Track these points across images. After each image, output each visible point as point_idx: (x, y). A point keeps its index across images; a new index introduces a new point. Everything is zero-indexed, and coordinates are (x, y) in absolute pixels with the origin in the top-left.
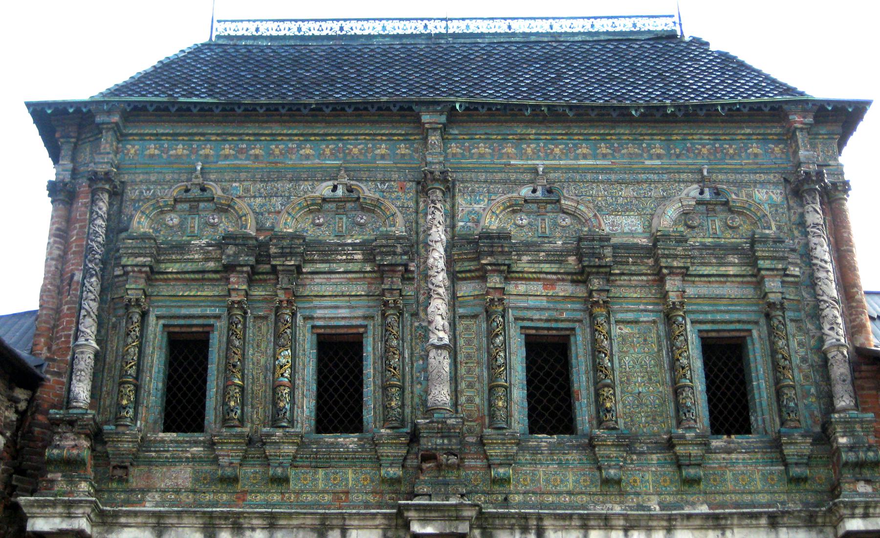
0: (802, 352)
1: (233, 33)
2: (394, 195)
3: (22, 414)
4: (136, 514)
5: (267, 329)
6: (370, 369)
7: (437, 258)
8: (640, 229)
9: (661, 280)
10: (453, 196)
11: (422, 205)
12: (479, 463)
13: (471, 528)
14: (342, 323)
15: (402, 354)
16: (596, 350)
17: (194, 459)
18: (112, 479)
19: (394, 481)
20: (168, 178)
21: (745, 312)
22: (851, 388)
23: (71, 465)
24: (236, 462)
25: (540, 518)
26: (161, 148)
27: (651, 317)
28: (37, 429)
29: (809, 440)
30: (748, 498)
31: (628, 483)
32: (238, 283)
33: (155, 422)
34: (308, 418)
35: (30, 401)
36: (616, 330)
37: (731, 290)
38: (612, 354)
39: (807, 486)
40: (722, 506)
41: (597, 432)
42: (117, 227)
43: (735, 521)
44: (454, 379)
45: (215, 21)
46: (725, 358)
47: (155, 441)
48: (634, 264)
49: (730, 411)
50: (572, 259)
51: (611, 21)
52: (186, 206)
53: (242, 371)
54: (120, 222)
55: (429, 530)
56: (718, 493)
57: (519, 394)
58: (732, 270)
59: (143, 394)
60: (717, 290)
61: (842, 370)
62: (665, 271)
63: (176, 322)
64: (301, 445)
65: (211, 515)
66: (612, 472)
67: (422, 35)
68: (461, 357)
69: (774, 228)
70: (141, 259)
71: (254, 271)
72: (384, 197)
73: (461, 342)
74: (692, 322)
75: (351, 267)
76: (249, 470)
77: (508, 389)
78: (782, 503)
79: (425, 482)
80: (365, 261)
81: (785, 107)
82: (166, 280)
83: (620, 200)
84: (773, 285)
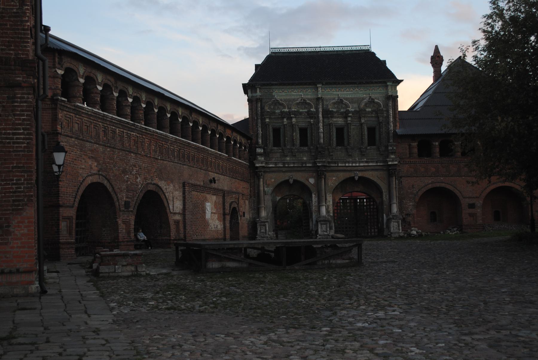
6: (309, 135)
7: (320, 115)
9: (360, 118)
16: (348, 132)
17: (280, 152)
23: (261, 154)
35: (251, 142)
36: (352, 127)
37: (374, 119)
42: (262, 108)
46: (371, 131)
49: (372, 141)
57: (335, 139)
84: (381, 119)
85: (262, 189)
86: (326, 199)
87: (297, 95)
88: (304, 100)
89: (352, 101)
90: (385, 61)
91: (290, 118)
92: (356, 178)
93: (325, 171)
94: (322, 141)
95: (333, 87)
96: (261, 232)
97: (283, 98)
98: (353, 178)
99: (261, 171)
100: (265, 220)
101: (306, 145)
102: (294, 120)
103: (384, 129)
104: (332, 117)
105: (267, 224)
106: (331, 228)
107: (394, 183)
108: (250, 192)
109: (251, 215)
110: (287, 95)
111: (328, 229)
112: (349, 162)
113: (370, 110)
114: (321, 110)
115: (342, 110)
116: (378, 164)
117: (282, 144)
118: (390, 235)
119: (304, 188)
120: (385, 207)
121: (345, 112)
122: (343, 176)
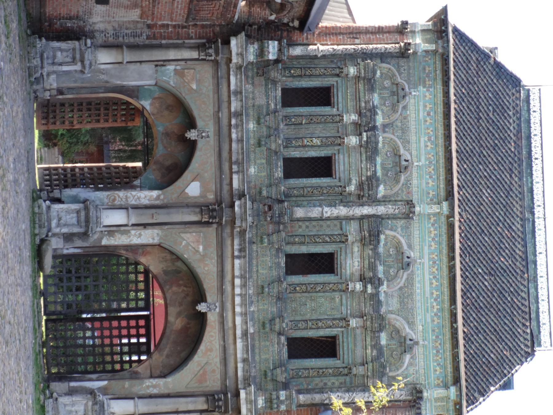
0: (329, 384)
1: (531, 98)
2: (404, 189)
3: (287, 24)
4: (241, 81)
5: (333, 133)
8: (390, 309)
10: (405, 218)
11: (400, 203)
12: (270, 231)
13: (240, 227)
14: (337, 167)
15: (322, 195)
17: (268, 104)
18: (258, 69)
19: (260, 193)
20: (411, 79)
21: (348, 357)
22: (309, 402)
23: (262, 52)
24: (267, 123)
25: (244, 257)
26: (430, 72)
27: (344, 312)
28: (280, 33)
29: (284, 380)
30: (257, 351)
31: (263, 297)
32: (354, 117)
33: (286, 85)
34: (290, 154)
35: (294, 28)
36: (337, 295)
37: (359, 352)
38: (324, 292)
39: (263, 379)
40: (253, 339)
41: (285, 283)
43: (246, 343)
44: (310, 219)
45: (539, 87)
46: (327, 347)
47: (276, 86)
48: (370, 304)
49: (301, 348)
50: (371, 274)
51: (547, 311)
52: (395, 89)
53: (310, 123)
54: (387, 58)
55: (237, 209)
56: (259, 338)
57: (304, 249)
58: (369, 351)
59: (298, 79)
60: (359, 345)
61: (317, 399)
62: (365, 318)
63: (335, 90)
64: (276, 153)
65: (242, 115)
66: (267, 290)
67: (533, 204)
68: (321, 223)
69: (391, 374)
70: (363, 71)
71: (360, 125)
72: (403, 185)
73: (328, 222)
74: (343, 332)
75: (364, 170)
76: (264, 129)
77: (302, 243)
78: (255, 367)
79: (259, 207)
80: (367, 177)
81: (459, 384)
82: (356, 83)
83: (406, 300)
84: (360, 370)
85: (172, 54)
86: (145, 226)
87: (418, 149)
88: (406, 168)
89: (406, 295)
90: (508, 386)
91: (358, 129)
92: (202, 307)
93: (220, 224)
94: (300, 213)
95: (440, 244)
96: (55, 50)
97: (411, 112)
98: (201, 297)
99: (217, 53)
100: (87, 63)
101: (288, 175)
102: (353, 140)
103: (333, 379)
104: (363, 241)
105: (78, 67)
106: (68, 238)
107: (191, 407)
108: (163, 26)
109: (100, 26)
110: (418, 124)
111: (65, 230)
112: (244, 286)
113: (383, 342)
114: (381, 210)
115: (380, 268)
116: (240, 365)
117: (290, 110)
118: (51, 396)
119: (174, 172)
120: (127, 384)
121: (375, 275)
122: (207, 272)
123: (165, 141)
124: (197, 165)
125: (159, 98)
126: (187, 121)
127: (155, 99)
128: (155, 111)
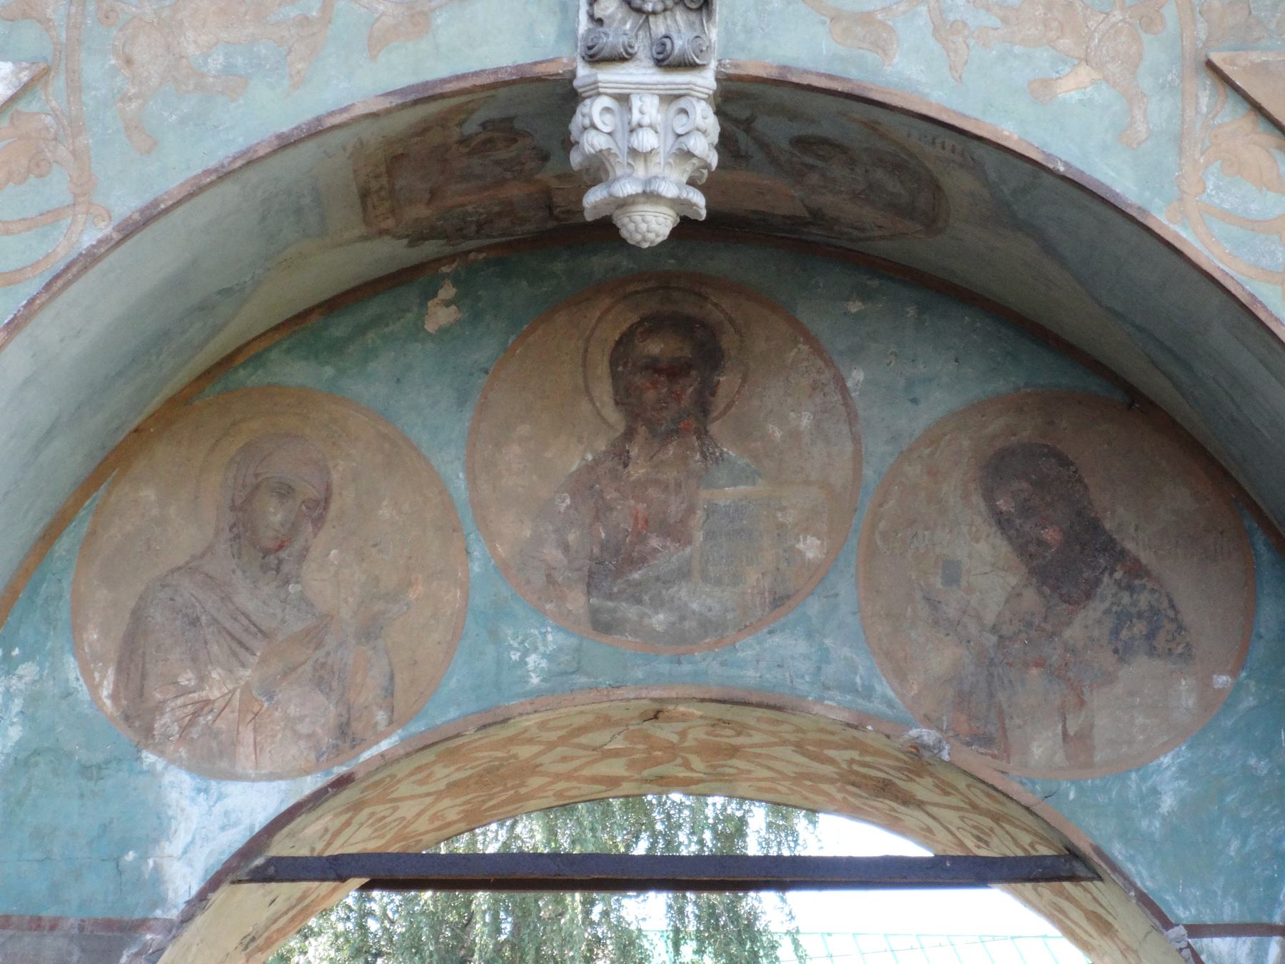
123: (699, 599)
124: (1075, 86)
125: (132, 659)
126: (440, 315)
127: (138, 716)
128: (311, 711)
